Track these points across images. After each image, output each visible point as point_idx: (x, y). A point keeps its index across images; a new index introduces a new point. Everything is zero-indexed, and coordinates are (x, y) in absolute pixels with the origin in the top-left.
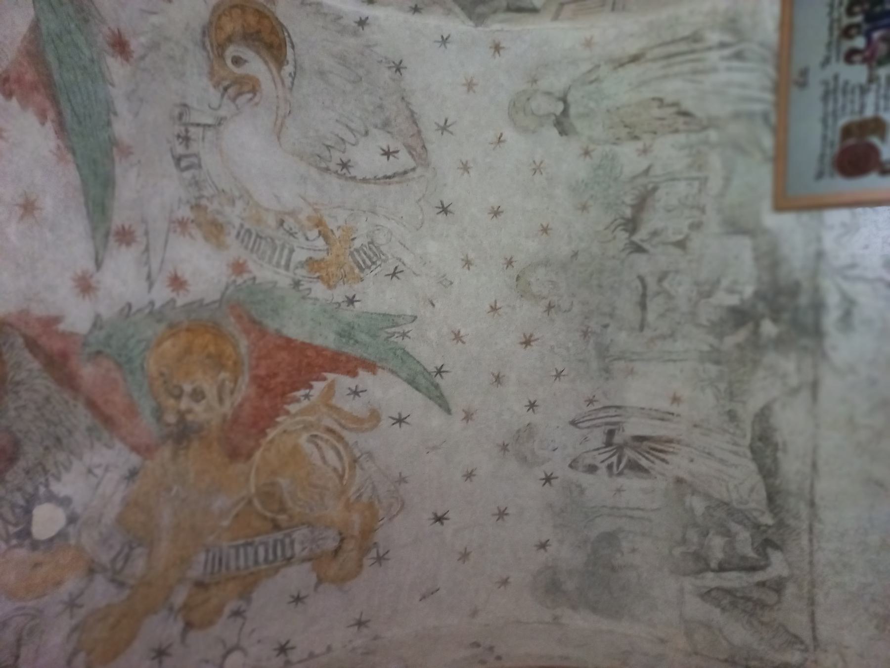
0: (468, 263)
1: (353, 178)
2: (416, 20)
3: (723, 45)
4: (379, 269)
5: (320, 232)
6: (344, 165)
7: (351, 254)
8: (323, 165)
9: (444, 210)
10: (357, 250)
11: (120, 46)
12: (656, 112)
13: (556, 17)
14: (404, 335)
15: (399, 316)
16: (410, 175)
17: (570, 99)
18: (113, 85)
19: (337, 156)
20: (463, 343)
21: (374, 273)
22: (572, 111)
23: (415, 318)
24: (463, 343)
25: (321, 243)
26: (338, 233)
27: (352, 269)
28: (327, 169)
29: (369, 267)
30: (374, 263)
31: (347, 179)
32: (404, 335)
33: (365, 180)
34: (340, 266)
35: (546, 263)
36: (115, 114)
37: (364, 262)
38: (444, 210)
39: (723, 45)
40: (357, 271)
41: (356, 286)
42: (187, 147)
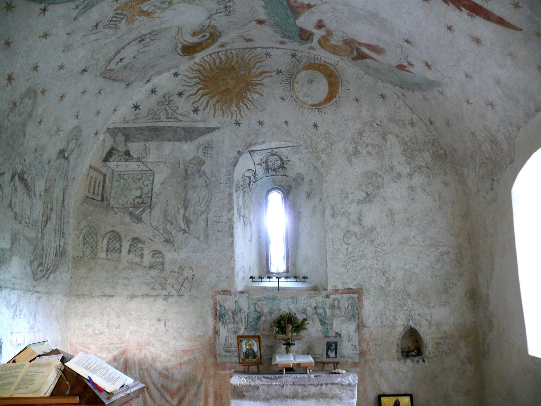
0: (61, 67)
1: (135, 40)
2: (130, 103)
3: (60, 246)
4: (106, 21)
5: (147, 11)
6: (143, 40)
7: (125, 15)
8: (154, 33)
9: (84, 71)
10: (122, 19)
11: (261, 22)
12: (50, 206)
13: (91, 167)
14: (77, 7)
15: (85, 12)
16: (107, 63)
17: (66, 161)
18: (264, 13)
19: (147, 40)
20: (40, 37)
21: (109, 17)
22: (62, 160)
23: (75, 19)
24: (40, 37)
25: (145, 9)
26: (136, 17)
27: (123, 10)
28: (150, 33)
29: (113, 17)
30: (111, 21)
31: (139, 37)
32: (77, 7)
33: (129, 44)
34: (130, 7)
35: (30, 115)
36: (263, 6)
37: (117, 17)
38: (84, 71)
39: (60, 246)
40: (120, 11)
41: (118, 5)
42: (226, 6)
